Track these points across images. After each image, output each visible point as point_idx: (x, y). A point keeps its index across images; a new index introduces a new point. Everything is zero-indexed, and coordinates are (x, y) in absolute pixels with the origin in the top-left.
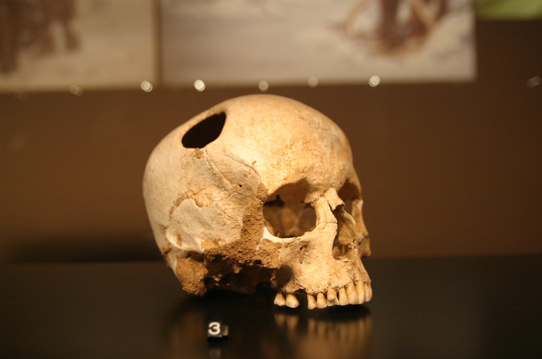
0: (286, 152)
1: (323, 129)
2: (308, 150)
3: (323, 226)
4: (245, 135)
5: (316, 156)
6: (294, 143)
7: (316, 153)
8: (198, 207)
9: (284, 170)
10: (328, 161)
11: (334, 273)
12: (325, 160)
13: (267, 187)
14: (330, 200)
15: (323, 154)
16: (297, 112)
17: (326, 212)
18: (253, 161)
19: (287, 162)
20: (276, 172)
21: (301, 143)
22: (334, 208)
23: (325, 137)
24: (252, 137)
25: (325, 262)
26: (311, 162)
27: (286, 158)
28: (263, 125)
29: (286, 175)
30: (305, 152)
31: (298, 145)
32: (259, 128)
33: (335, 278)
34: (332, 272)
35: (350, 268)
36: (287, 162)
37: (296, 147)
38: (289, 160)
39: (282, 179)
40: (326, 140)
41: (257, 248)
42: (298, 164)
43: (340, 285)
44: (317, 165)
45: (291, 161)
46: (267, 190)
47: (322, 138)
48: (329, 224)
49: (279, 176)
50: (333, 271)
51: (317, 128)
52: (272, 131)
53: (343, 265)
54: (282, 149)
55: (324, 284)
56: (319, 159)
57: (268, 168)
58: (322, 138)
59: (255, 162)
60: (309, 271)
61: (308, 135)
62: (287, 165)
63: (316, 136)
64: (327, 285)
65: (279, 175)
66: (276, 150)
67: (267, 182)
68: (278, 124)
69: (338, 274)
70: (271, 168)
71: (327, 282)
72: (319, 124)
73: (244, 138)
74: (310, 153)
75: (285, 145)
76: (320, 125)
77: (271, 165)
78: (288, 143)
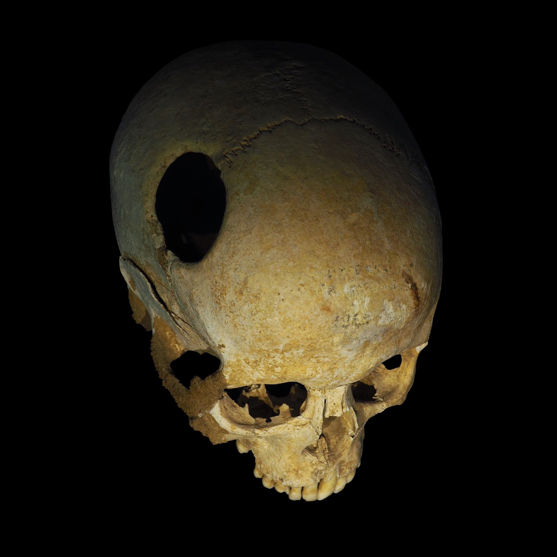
0: (272, 355)
1: (358, 326)
2: (312, 357)
3: (303, 422)
4: (223, 304)
5: (324, 363)
6: (290, 349)
7: (326, 359)
8: (153, 296)
9: (261, 372)
10: (347, 365)
11: (294, 470)
12: (340, 365)
13: (227, 382)
14: (328, 401)
15: (341, 359)
16: (326, 290)
17: (316, 410)
18: (221, 344)
19: (270, 366)
20: (250, 369)
21: (301, 351)
22: (327, 416)
23: (356, 338)
24: (231, 315)
25: (287, 456)
26: (309, 371)
27: (271, 361)
28: (253, 306)
29: (262, 377)
30: (305, 360)
31: (295, 352)
32: (246, 307)
33: (292, 475)
34: (291, 469)
35: (320, 468)
36: (270, 366)
37: (292, 353)
38: (273, 364)
39: (255, 379)
40: (355, 342)
41: (200, 415)
42: (286, 373)
43: (296, 486)
44: (318, 376)
45: (277, 367)
46: (226, 385)
47: (346, 341)
48: (311, 427)
49: (251, 375)
50: (294, 467)
51: (346, 327)
52: (262, 325)
53: (314, 463)
54: (267, 351)
55: (275, 475)
56: (326, 367)
57: (239, 361)
58: (346, 341)
59: (223, 346)
60: (266, 447)
61: (322, 341)
62: (268, 369)
63: (336, 339)
64: (278, 479)
65: (253, 374)
66: (259, 349)
67: (230, 376)
68: (276, 318)
69: (300, 472)
70: (243, 363)
71: (278, 476)
72: (356, 315)
73: (220, 308)
74: (314, 360)
75: (274, 348)
76: (359, 317)
77: (245, 360)
78: (281, 347)
